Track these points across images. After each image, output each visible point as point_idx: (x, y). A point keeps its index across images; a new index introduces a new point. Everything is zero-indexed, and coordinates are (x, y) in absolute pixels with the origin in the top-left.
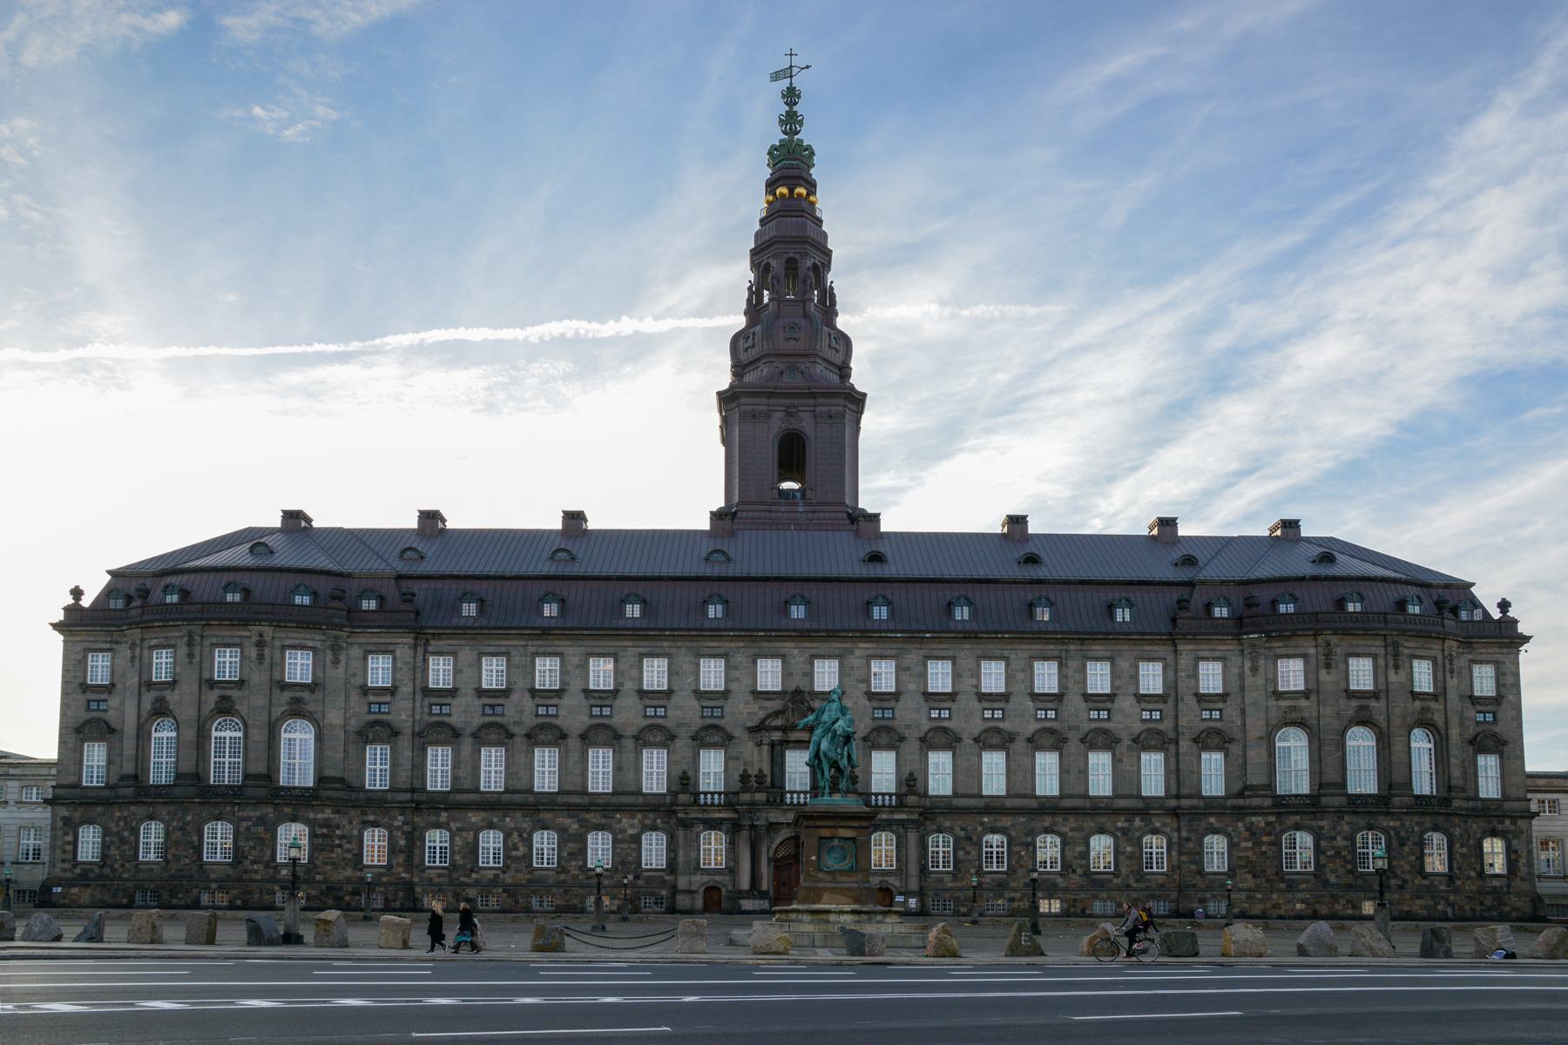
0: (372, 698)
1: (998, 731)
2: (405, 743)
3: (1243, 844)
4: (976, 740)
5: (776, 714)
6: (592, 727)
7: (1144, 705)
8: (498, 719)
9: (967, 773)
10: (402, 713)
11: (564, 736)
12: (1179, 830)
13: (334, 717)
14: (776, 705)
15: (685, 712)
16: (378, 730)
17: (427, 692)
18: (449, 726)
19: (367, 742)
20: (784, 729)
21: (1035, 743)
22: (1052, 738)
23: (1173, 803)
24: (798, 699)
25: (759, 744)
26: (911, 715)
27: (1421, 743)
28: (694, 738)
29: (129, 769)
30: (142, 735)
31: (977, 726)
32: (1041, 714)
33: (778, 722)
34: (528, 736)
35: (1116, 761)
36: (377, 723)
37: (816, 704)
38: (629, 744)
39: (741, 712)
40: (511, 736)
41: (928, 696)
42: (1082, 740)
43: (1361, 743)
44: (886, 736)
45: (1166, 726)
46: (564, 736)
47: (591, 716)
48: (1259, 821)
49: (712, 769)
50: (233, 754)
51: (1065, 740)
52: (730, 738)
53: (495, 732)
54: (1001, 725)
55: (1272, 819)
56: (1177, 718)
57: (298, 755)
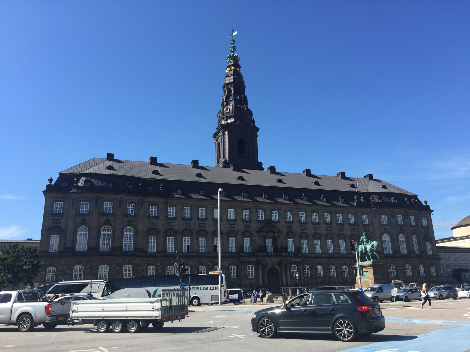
13: (140, 227)
15: (240, 226)
18: (173, 229)
21: (327, 237)
22: (329, 236)
26: (296, 228)
27: (414, 239)
33: (265, 230)
34: (197, 233)
36: (153, 228)
37: (273, 224)
39: (254, 226)
40: (192, 233)
43: (402, 238)
45: (356, 233)
46: (207, 233)
49: (247, 242)
50: (108, 239)
51: (333, 237)
52: (252, 234)
53: (186, 232)
56: (358, 231)
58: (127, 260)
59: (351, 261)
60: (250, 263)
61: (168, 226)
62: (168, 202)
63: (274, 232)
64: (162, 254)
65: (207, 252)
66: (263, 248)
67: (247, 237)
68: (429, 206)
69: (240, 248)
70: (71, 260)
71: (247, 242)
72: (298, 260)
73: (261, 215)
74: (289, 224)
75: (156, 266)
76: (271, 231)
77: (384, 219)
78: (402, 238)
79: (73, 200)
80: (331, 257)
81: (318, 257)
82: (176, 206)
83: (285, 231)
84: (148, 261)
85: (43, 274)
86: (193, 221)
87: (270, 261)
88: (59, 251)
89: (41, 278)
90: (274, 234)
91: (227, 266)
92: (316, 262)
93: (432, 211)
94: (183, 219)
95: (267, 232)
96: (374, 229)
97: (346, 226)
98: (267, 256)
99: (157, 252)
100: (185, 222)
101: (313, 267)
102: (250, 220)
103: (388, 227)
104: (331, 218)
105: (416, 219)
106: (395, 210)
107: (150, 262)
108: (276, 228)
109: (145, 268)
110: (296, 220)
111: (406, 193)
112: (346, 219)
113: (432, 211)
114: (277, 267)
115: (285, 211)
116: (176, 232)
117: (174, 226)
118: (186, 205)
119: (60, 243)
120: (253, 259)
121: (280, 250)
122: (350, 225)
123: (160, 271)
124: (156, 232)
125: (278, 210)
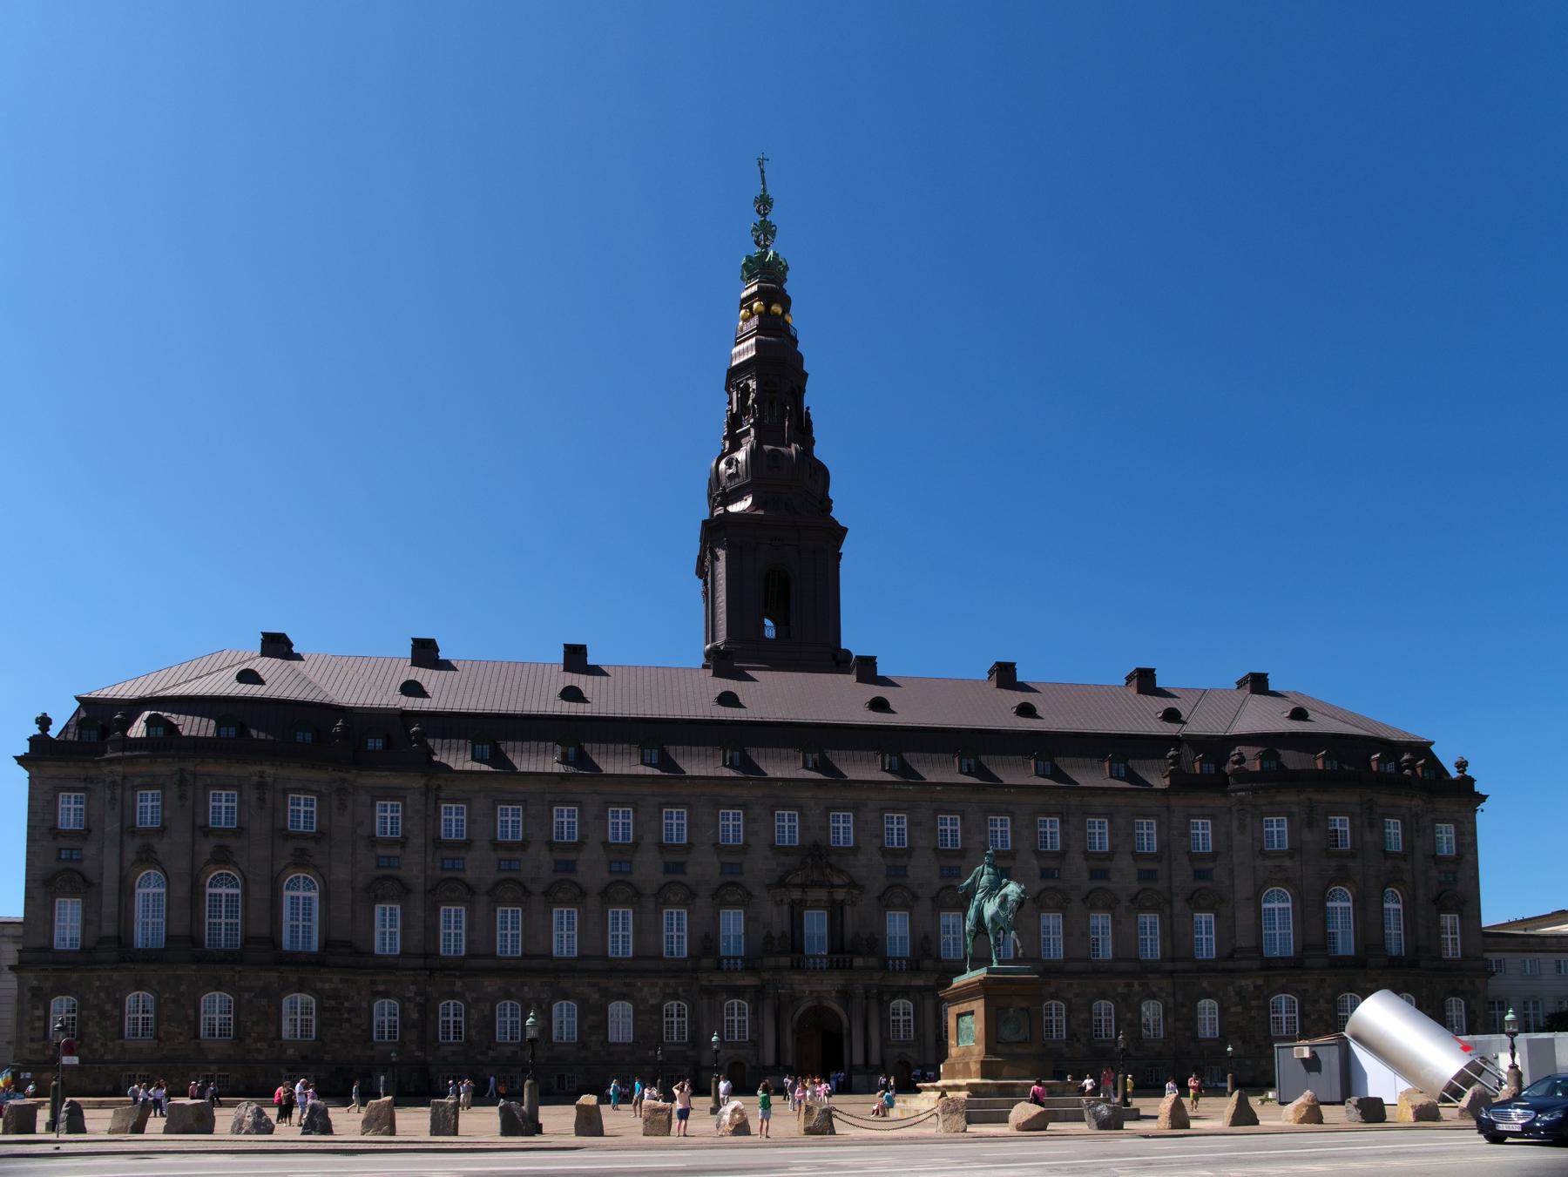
0: (380, 851)
3: (1233, 1009)
6: (611, 883)
8: (513, 875)
10: (413, 867)
11: (583, 894)
12: (1174, 995)
15: (704, 868)
16: (388, 886)
17: (438, 844)
19: (378, 899)
23: (1169, 966)
24: (816, 859)
25: (779, 903)
29: (109, 929)
30: (126, 891)
33: (798, 880)
34: (546, 893)
35: (1116, 923)
40: (528, 893)
43: (1341, 904)
48: (1247, 983)
49: (732, 924)
52: (750, 895)
53: (511, 889)
55: (1260, 982)
57: (301, 915)
58: (293, 978)
59: (1129, 986)
60: (737, 992)
61: (443, 869)
63: (832, 886)
64: (420, 962)
65: (581, 957)
66: (794, 943)
67: (733, 905)
68: (1471, 781)
69: (706, 944)
70: (115, 975)
71: (732, 924)
72: (918, 982)
73: (788, 827)
74: (897, 860)
75: (402, 1000)
76: (819, 885)
77: (1278, 831)
78: (1341, 904)
79: (114, 783)
82: (468, 801)
84: (373, 983)
85: (39, 1018)
87: (805, 987)
88: (83, 949)
89: (33, 1029)
91: (652, 1001)
93: (1483, 798)
94: (496, 845)
95: (803, 886)
96: (1231, 872)
98: (797, 967)
99: (403, 954)
100: (502, 854)
102: (746, 844)
103: (1287, 863)
104: (1065, 834)
105: (1409, 830)
106: (1326, 797)
107: (381, 988)
108: (841, 872)
109: (365, 1005)
111: (1384, 734)
113: (1483, 798)
114: (835, 1007)
115: (883, 810)
116: (471, 890)
117: (463, 870)
119: (86, 922)
120: (750, 980)
122: (1137, 857)
123: (415, 1016)
124: (401, 890)
125: (856, 808)
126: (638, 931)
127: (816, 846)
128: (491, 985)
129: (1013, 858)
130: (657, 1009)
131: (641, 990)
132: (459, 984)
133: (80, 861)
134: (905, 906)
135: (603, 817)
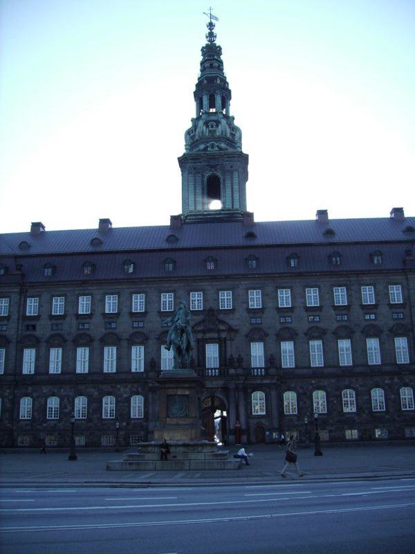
1: (317, 328)
2: (12, 346)
4: (305, 334)
5: (199, 324)
6: (106, 335)
7: (394, 310)
8: (59, 332)
9: (302, 354)
14: (199, 318)
20: (204, 332)
21: (338, 335)
22: (347, 332)
28: (158, 339)
31: (306, 326)
32: (339, 318)
33: (201, 328)
34: (74, 341)
35: (381, 344)
37: (221, 317)
38: (124, 343)
40: (65, 341)
41: (279, 310)
42: (362, 332)
44: (257, 334)
47: (106, 329)
51: (353, 332)
54: (318, 325)
56: (411, 316)
62: (27, 291)
63: (219, 331)
64: (10, 378)
73: (196, 301)
80: (347, 373)
81: (317, 373)
82: (39, 296)
83: (245, 329)
86: (68, 319)
90: (219, 334)
91: (125, 396)
92: (312, 384)
94: (52, 317)
95: (204, 332)
97: (384, 310)
100: (54, 322)
101: (306, 393)
104: (349, 296)
110: (270, 305)
112: (382, 295)
115: (247, 289)
118: (59, 293)
121: (233, 363)
125: (233, 289)
126: (119, 358)
127: (211, 310)
128: (45, 390)
129: (321, 311)
130: (128, 401)
131: (119, 389)
132: (30, 388)
133: (62, 330)
134: (260, 340)
135: (103, 300)
